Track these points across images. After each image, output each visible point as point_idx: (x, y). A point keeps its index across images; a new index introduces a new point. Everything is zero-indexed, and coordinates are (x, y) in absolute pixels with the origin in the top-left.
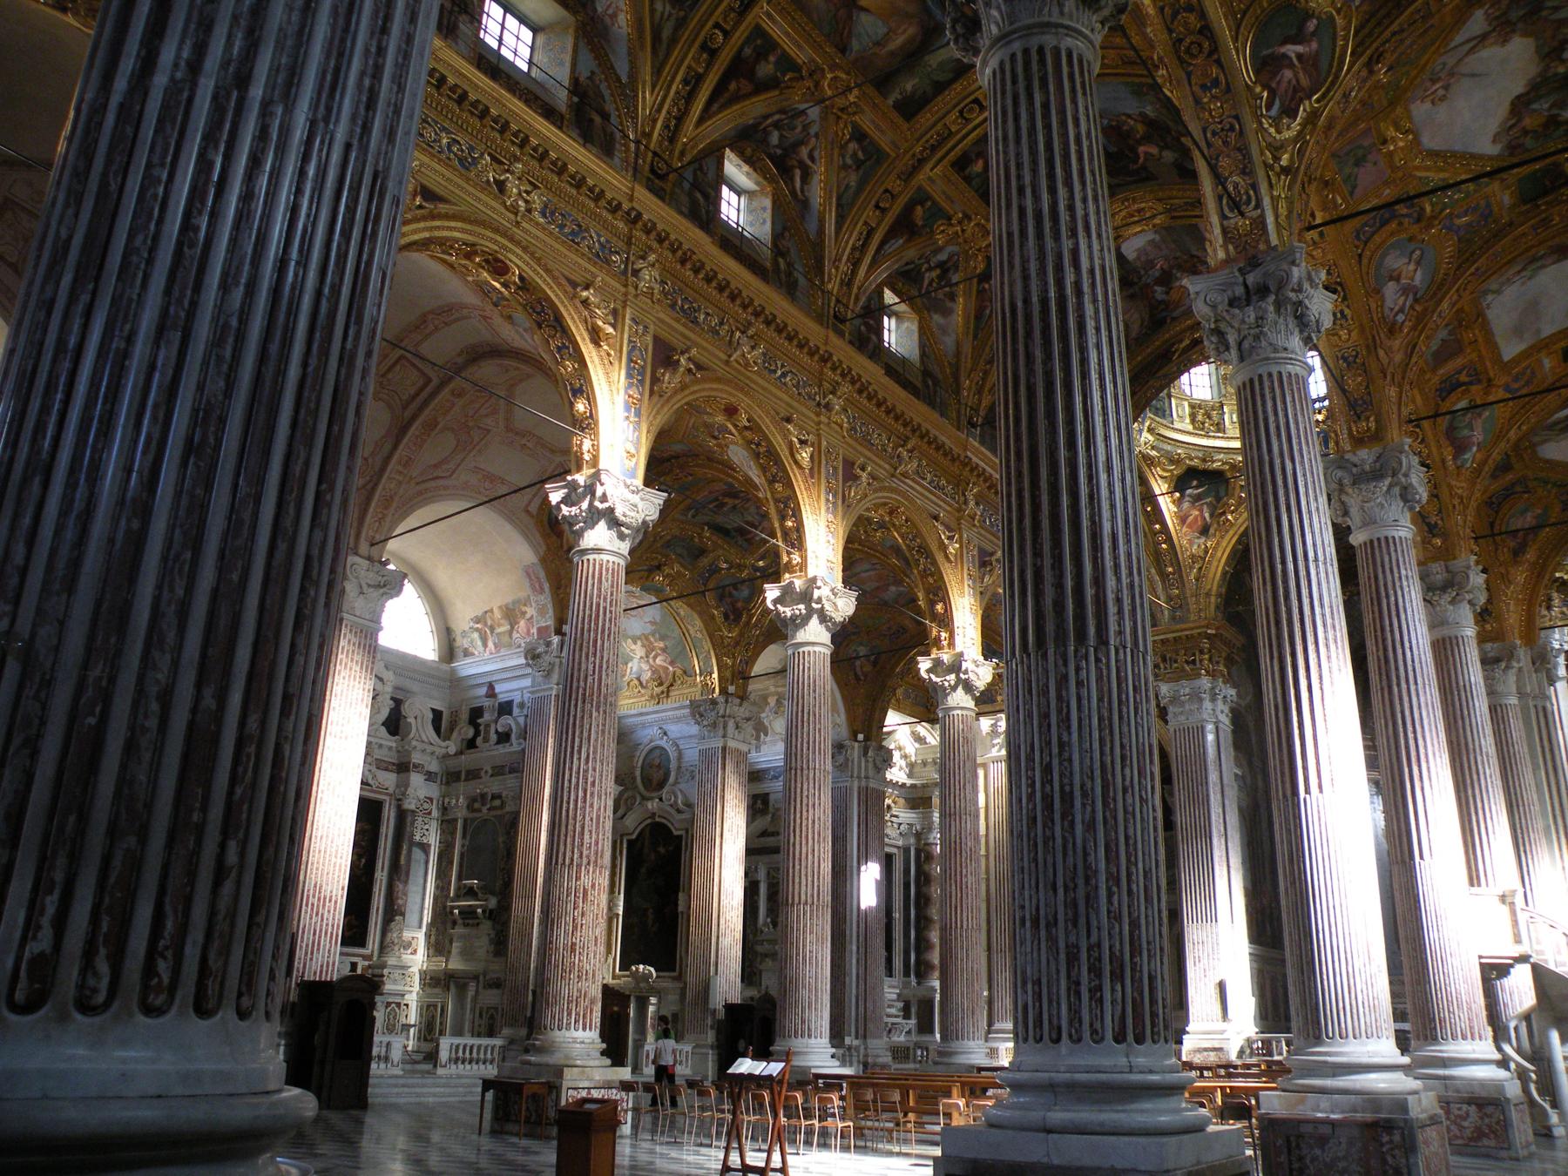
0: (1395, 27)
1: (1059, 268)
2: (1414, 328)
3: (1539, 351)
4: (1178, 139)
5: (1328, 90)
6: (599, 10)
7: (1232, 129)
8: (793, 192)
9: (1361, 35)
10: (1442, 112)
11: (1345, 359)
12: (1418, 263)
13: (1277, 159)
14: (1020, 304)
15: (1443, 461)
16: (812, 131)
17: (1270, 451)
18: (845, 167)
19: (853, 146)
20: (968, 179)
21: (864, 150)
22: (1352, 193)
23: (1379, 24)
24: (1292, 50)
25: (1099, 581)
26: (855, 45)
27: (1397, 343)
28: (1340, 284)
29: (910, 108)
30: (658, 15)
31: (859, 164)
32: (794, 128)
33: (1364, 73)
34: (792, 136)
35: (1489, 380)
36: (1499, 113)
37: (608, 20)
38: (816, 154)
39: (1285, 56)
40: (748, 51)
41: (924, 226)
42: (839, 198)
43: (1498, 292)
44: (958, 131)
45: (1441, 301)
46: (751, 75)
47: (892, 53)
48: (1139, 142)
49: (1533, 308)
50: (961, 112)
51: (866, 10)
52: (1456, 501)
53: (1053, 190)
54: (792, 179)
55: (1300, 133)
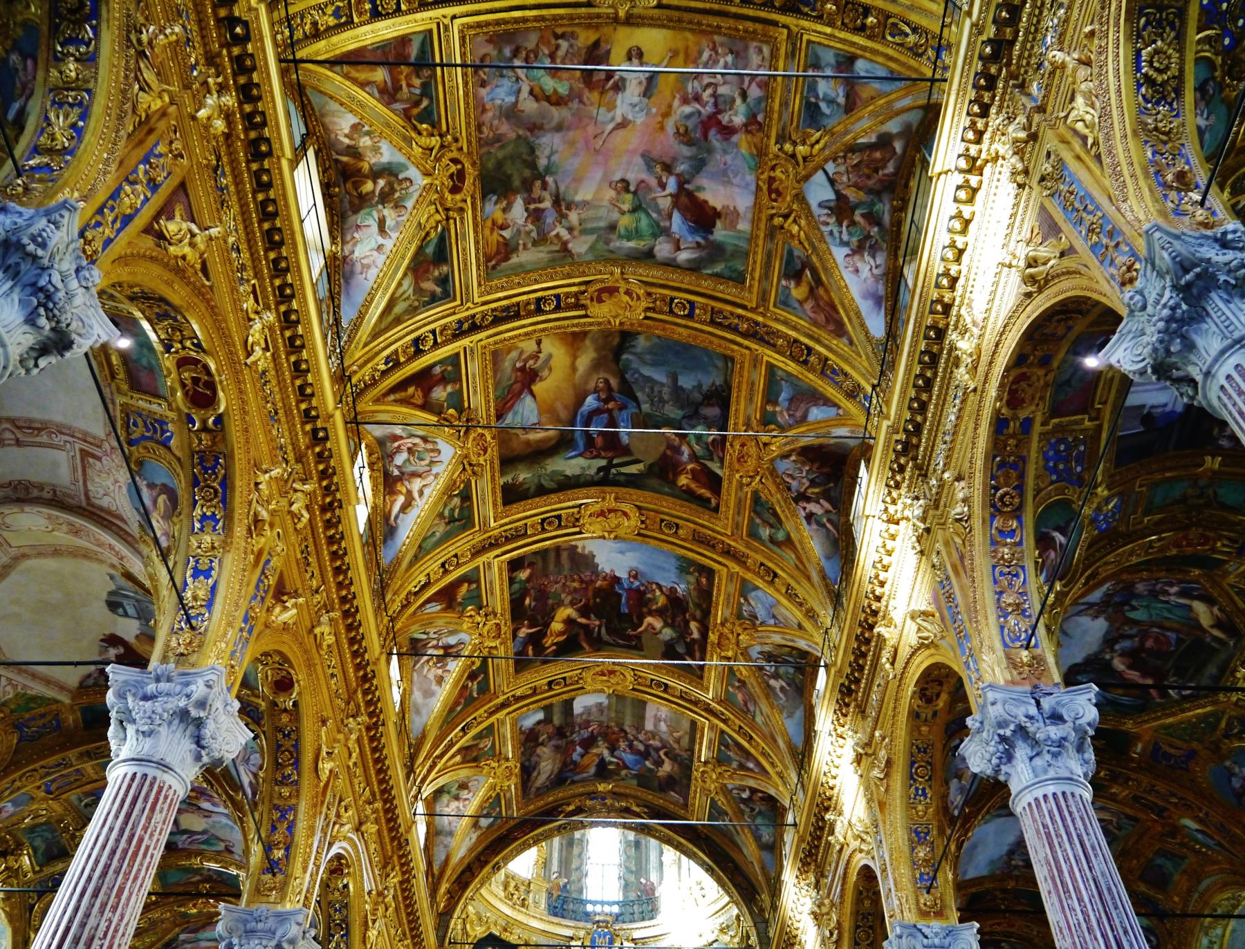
4: (687, 623)
6: (357, 254)
7: (1017, 575)
8: (387, 517)
9: (1091, 551)
11: (917, 833)
16: (435, 470)
18: (441, 515)
19: (456, 501)
20: (512, 581)
21: (461, 508)
23: (1098, 550)
26: (509, 419)
29: (512, 495)
30: (401, 291)
31: (452, 520)
32: (422, 460)
34: (421, 466)
37: (358, 268)
38: (427, 492)
39: (1053, 539)
40: (438, 370)
41: (460, 604)
42: (425, 539)
44: (534, 535)
46: (427, 392)
47: (528, 443)
48: (651, 613)
50: (543, 520)
51: (534, 396)
54: (393, 503)
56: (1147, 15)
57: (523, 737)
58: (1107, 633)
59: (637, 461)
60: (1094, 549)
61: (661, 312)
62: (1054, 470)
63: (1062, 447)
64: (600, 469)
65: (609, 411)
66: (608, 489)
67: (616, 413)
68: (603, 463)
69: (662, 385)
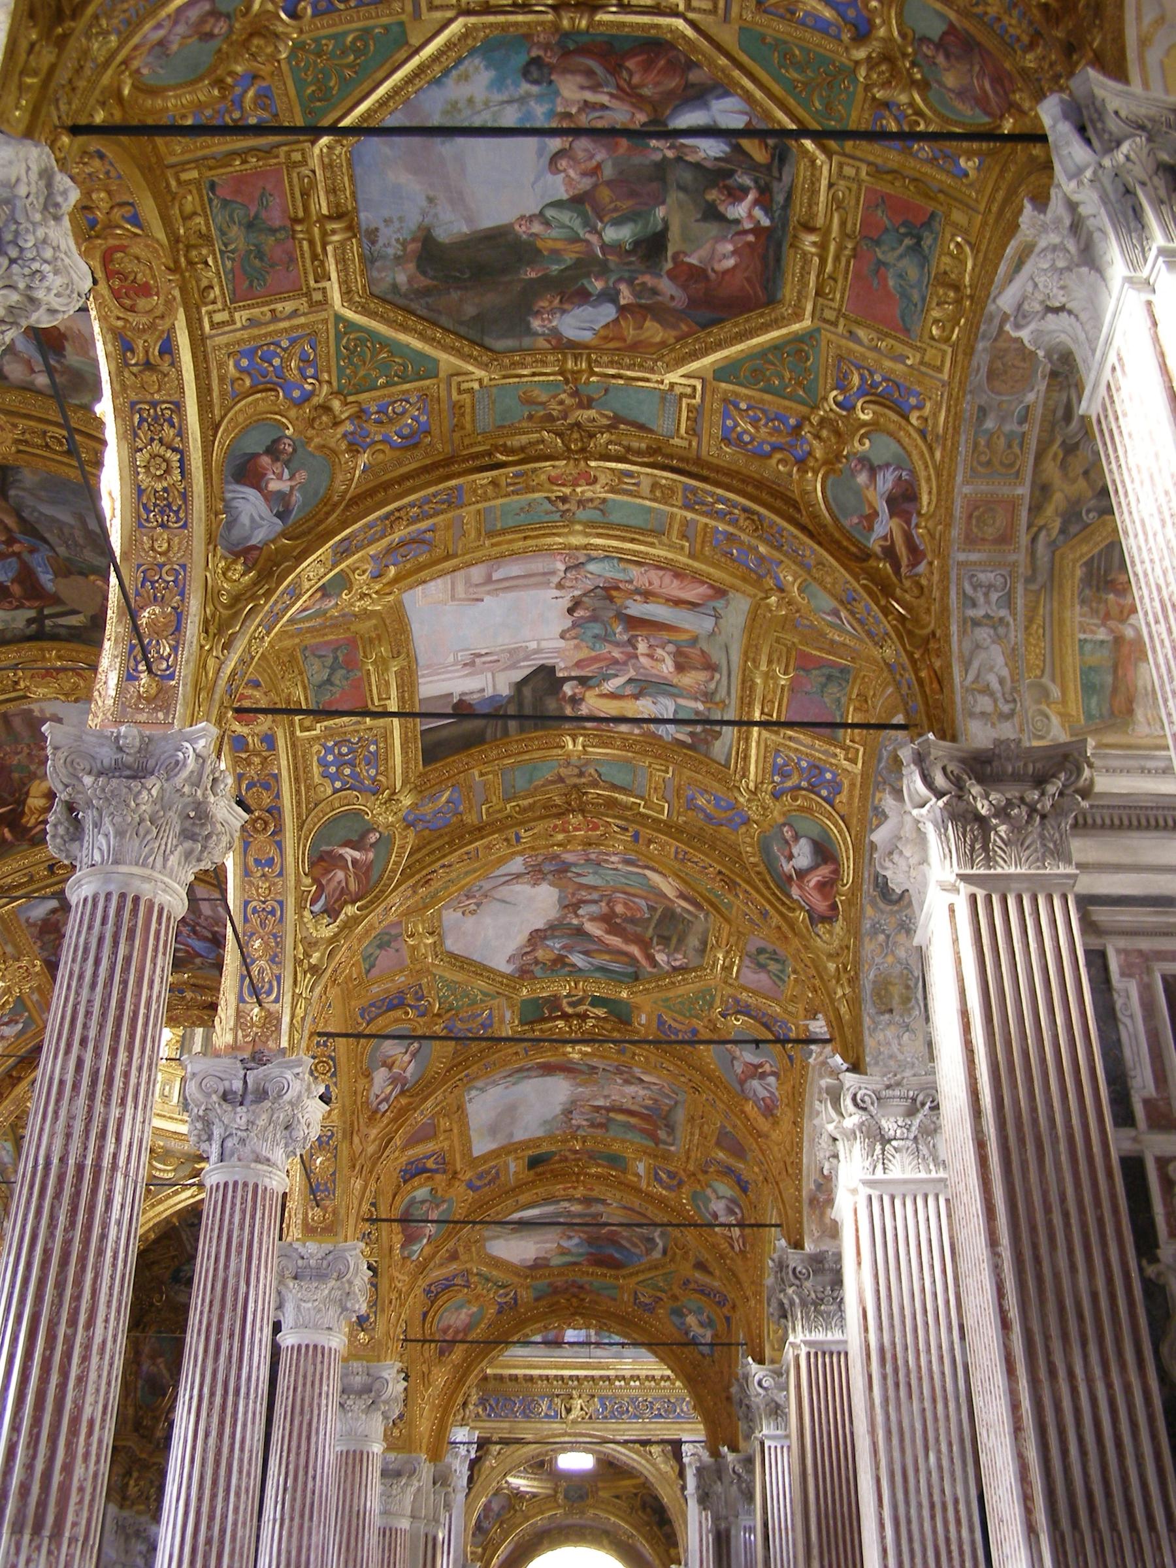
0: (446, 861)
1: (102, 1135)
2: (394, 1120)
3: (508, 1153)
5: (371, 902)
7: (273, 912)
9: (418, 856)
10: (469, 922)
12: (414, 1055)
13: (307, 955)
14: (55, 1161)
15: (391, 1249)
17: (226, 1267)
22: (368, 971)
24: (349, 853)
25: (68, 1469)
27: (374, 1132)
28: (333, 1059)
33: (410, 892)
35: (456, 1173)
36: (519, 938)
43: (482, 1090)
45: (425, 1099)
49: (510, 1111)
52: (394, 1296)
53: (114, 1052)
55: (336, 935)
56: (140, 411)
57: (35, 931)
58: (560, 900)
59: (74, 612)
60: (425, 851)
61: (38, 447)
62: (332, 778)
63: (345, 750)
64: (30, 621)
65: (17, 555)
66: (45, 644)
67: (26, 556)
68: (32, 614)
69: (72, 527)
